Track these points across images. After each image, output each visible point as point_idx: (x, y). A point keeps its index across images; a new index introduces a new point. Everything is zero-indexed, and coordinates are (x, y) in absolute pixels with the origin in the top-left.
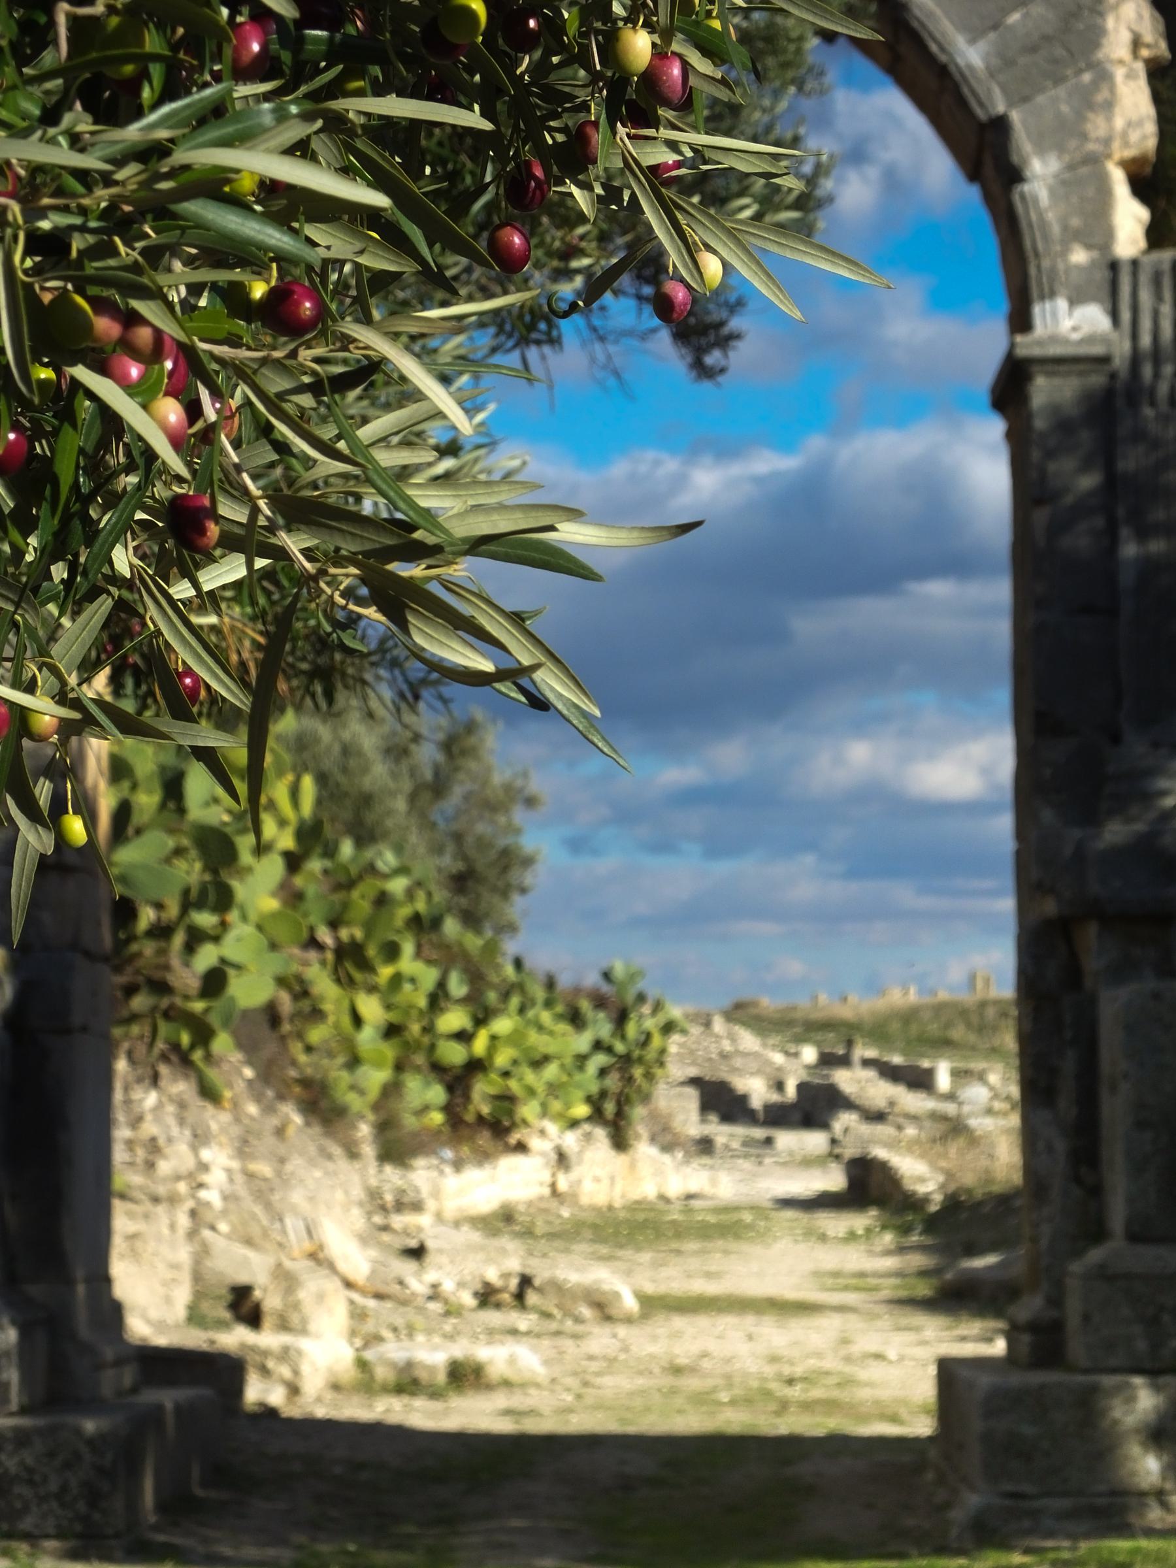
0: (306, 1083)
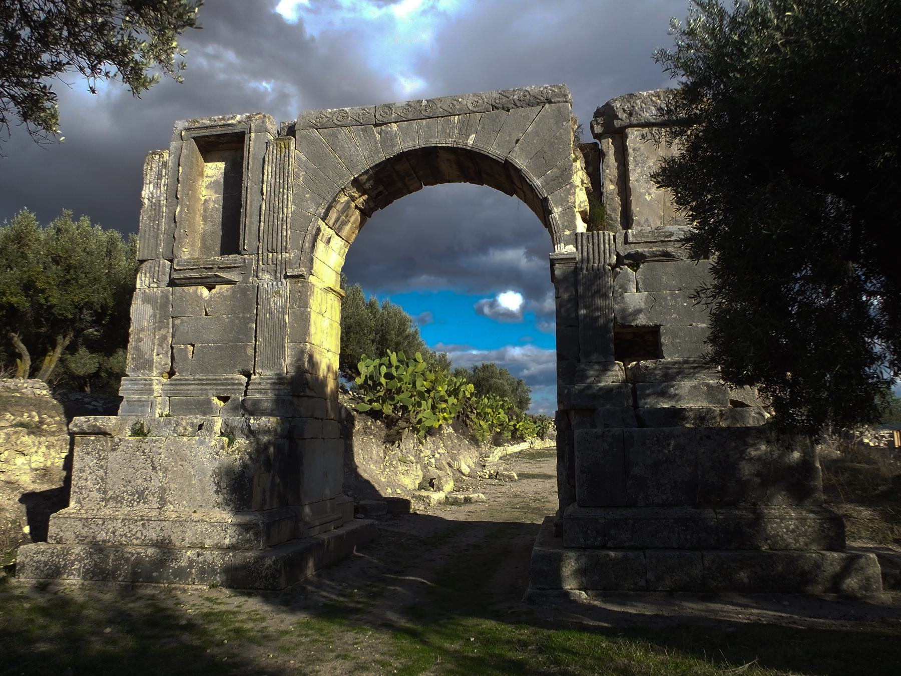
0: (472, 435)
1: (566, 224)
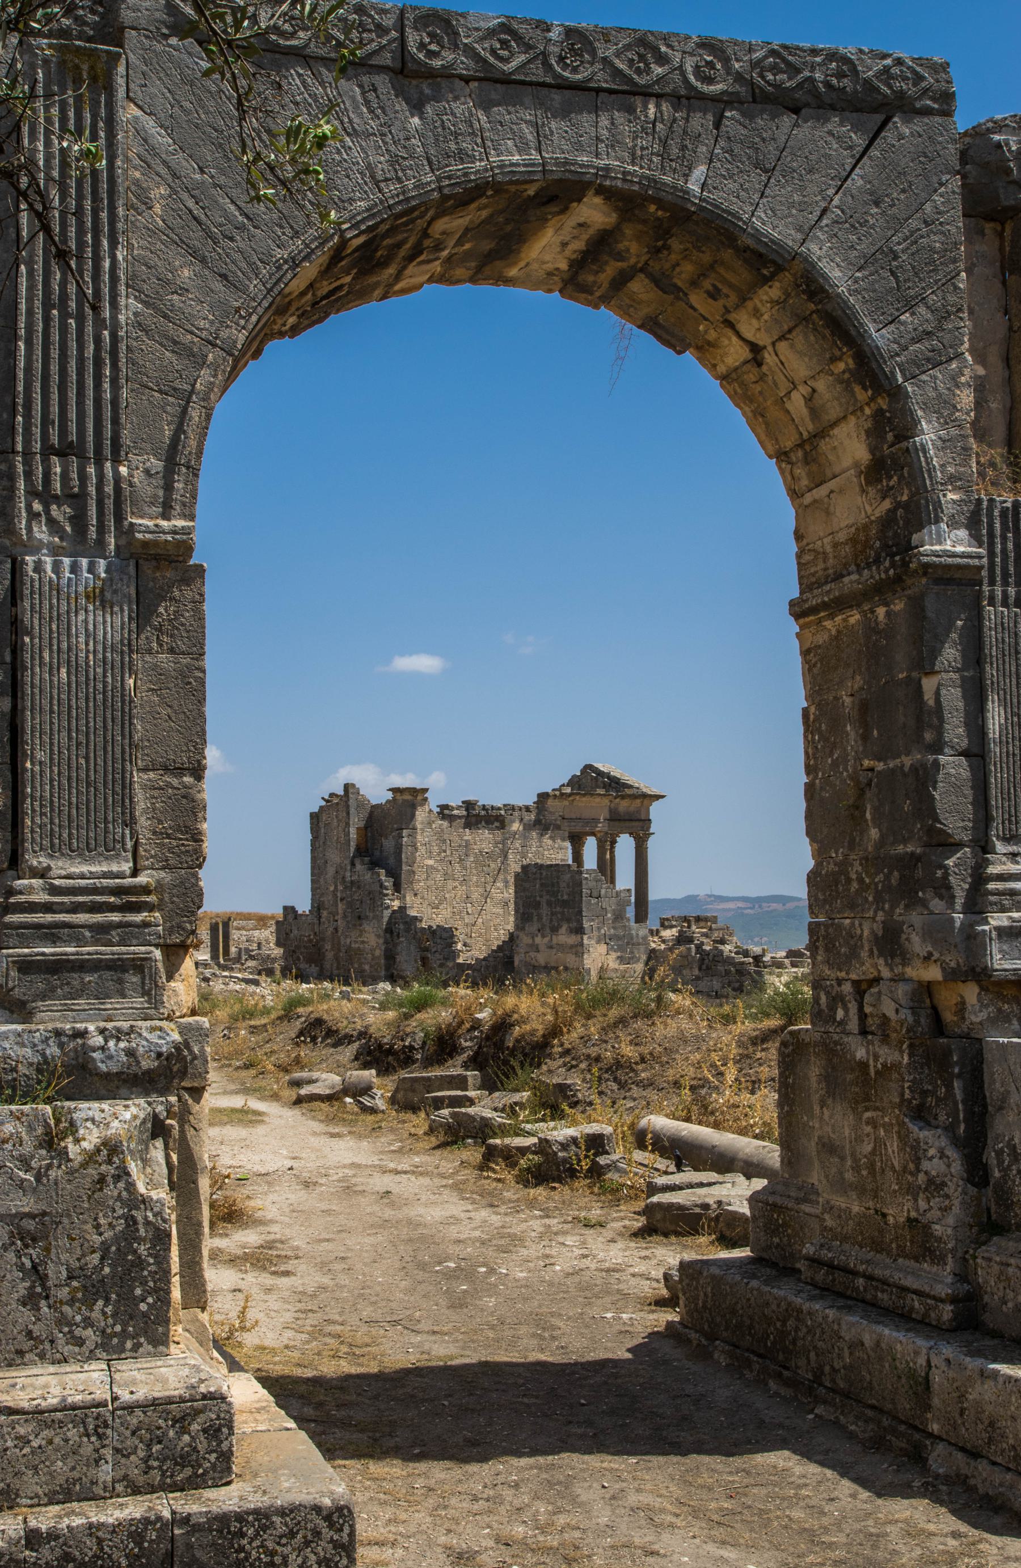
1: (951, 469)
